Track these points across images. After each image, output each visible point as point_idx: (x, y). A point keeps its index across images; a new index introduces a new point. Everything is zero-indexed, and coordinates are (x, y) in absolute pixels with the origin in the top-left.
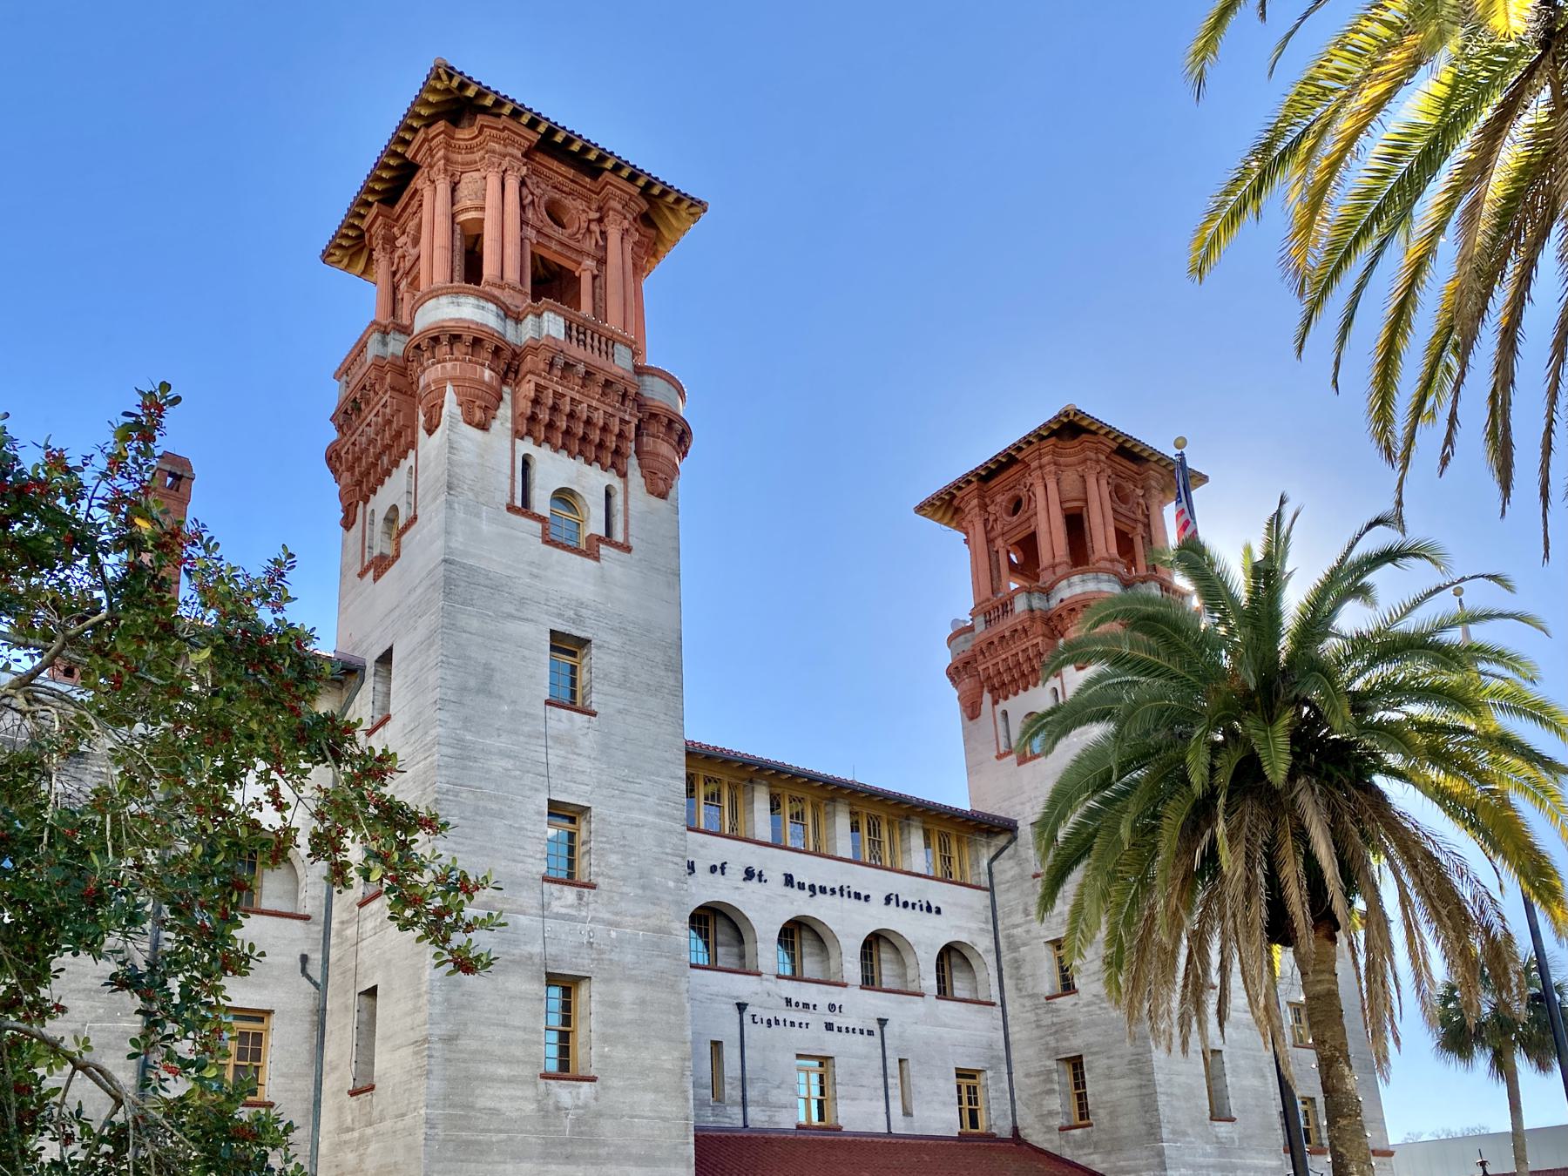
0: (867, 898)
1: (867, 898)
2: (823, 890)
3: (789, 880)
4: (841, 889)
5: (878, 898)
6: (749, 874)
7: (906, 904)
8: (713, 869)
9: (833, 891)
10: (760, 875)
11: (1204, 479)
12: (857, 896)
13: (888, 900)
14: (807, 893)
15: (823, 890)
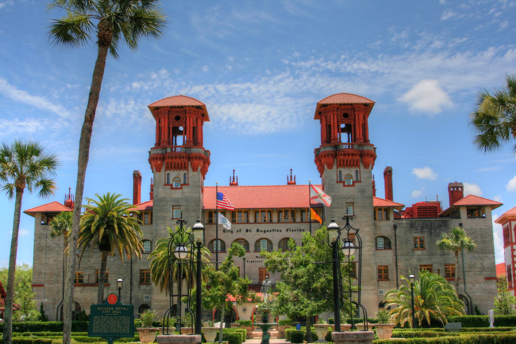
0: (281, 231)
1: (281, 231)
2: (268, 231)
3: (258, 230)
4: (273, 230)
5: (284, 230)
6: (247, 231)
7: (293, 231)
8: (238, 231)
9: (271, 231)
10: (250, 231)
11: (367, 107)
12: (278, 231)
13: (287, 230)
14: (263, 232)
15: (268, 231)
